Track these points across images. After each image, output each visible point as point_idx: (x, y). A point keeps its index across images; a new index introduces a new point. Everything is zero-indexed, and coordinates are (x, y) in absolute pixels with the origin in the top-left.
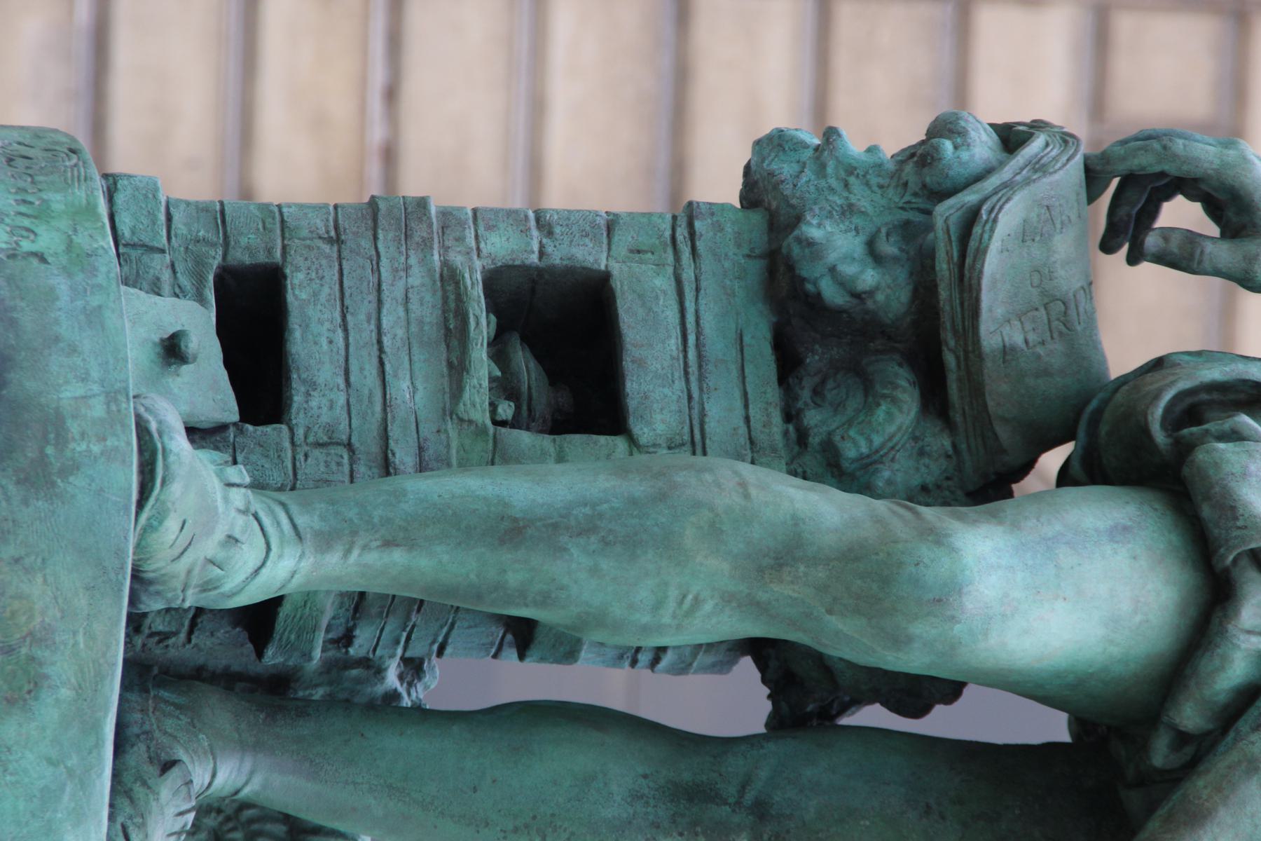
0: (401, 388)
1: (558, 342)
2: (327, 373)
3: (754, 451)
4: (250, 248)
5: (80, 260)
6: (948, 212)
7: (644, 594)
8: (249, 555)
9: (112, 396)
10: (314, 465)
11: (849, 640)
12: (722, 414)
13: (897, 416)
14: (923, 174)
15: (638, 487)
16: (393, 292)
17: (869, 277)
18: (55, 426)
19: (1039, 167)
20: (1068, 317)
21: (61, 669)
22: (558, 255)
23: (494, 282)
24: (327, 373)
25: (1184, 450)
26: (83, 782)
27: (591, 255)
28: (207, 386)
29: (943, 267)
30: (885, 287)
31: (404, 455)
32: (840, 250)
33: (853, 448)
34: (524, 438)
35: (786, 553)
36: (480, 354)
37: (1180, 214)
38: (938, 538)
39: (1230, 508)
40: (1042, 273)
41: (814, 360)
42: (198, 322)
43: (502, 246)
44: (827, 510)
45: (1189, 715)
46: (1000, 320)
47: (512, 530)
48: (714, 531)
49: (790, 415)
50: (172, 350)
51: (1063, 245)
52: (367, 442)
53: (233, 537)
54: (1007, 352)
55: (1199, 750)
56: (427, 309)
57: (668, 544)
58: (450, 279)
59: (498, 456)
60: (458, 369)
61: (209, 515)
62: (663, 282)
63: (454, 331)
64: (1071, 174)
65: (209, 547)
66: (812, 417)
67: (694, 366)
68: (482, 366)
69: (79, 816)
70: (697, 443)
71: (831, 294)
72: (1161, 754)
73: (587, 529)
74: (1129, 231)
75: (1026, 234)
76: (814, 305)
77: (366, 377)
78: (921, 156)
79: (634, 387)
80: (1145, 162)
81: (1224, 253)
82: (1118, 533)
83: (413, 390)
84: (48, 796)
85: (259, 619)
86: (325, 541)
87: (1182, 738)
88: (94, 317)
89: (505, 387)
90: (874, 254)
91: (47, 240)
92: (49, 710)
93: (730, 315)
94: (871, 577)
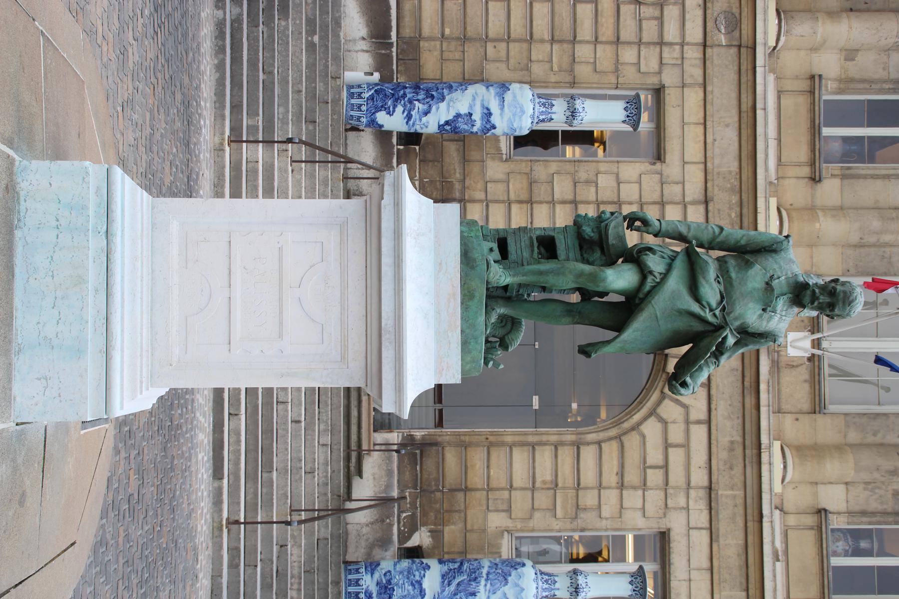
0: (524, 254)
1: (547, 246)
2: (514, 252)
3: (577, 260)
4: (502, 235)
5: (477, 237)
6: (603, 224)
7: (561, 281)
8: (503, 278)
9: (483, 255)
10: (512, 265)
11: (591, 287)
12: (571, 255)
13: (597, 254)
14: (600, 219)
15: (559, 266)
16: (523, 240)
17: (592, 235)
18: (475, 260)
19: (616, 217)
20: (622, 239)
21: (477, 294)
22: (547, 234)
23: (537, 238)
24: (514, 252)
25: (639, 257)
26: (481, 310)
27: (552, 234)
28: (496, 255)
29: (603, 233)
30: (595, 236)
31: (525, 263)
32: (588, 230)
33: (591, 259)
34: (543, 260)
35: (581, 274)
36: (536, 248)
37: (637, 223)
38: (603, 271)
39: (646, 265)
40: (618, 233)
41: (585, 247)
42: (495, 246)
43: (538, 233)
44: (587, 268)
45: (641, 295)
46: (612, 240)
47: (541, 273)
48: (570, 272)
49: (582, 255)
50: (491, 250)
51: (620, 229)
52: (520, 262)
53: (501, 276)
54: (613, 245)
55: (642, 300)
56: (528, 243)
57: (564, 274)
58: (531, 238)
59: (539, 263)
60: (533, 251)
61: (497, 272)
62: (562, 237)
63: (532, 245)
64: (621, 218)
65: (497, 277)
66: (585, 255)
67: (567, 249)
68: (536, 250)
69: (481, 315)
70: (568, 259)
71: (587, 237)
72: (637, 301)
73: (552, 272)
74: (630, 226)
75: (615, 227)
76: (584, 239)
77: (519, 252)
78: (599, 217)
79: (559, 252)
80: (632, 216)
81: (644, 229)
82: (629, 270)
83: (526, 254)
84: (476, 313)
85: (506, 288)
86: (514, 276)
87: (640, 299)
88: (479, 245)
89: (540, 253)
90: (593, 231)
91: (473, 234)
92: (476, 300)
93: (572, 241)
94: (594, 278)
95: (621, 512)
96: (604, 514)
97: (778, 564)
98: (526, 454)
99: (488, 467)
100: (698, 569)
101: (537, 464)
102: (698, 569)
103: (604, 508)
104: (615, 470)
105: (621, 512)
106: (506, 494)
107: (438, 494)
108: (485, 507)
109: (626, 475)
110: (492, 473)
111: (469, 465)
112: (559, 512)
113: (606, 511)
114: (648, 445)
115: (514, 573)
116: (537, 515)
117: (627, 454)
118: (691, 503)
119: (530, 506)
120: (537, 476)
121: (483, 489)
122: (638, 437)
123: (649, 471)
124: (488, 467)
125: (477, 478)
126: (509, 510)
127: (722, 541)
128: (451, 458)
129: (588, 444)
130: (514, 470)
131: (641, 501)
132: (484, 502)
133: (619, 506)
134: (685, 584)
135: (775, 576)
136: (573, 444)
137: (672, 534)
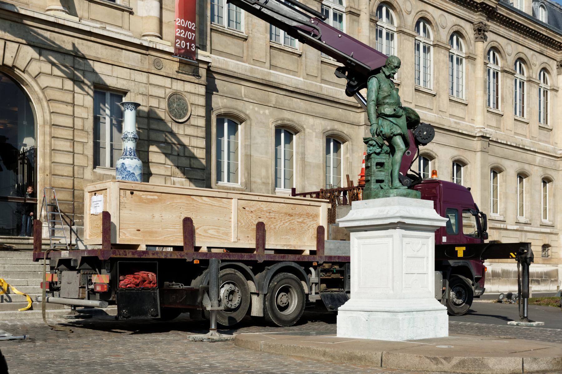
95: (85, 107)
96: (86, 117)
97: (107, 28)
98: (56, 155)
99: (62, 176)
100: (112, 72)
101: (61, 149)
102: (112, 72)
103: (83, 116)
104: (64, 106)
105: (85, 107)
106: (75, 168)
107: (75, 204)
108: (82, 180)
109: (68, 101)
110: (66, 174)
111: (61, 186)
112: (85, 140)
113: (85, 115)
114: (52, 85)
115: (128, 169)
116: (86, 152)
117: (57, 99)
118: (81, 68)
119: (82, 156)
120: (67, 150)
121: (74, 180)
122: (48, 90)
123: (65, 88)
124: (62, 176)
125: (68, 183)
126: (83, 167)
127: (99, 56)
128: (59, 196)
129: (51, 119)
130: (64, 162)
131: (80, 95)
132: (79, 180)
133: (82, 108)
134: (119, 80)
135: (118, 33)
136: (50, 128)
137: (96, 82)
